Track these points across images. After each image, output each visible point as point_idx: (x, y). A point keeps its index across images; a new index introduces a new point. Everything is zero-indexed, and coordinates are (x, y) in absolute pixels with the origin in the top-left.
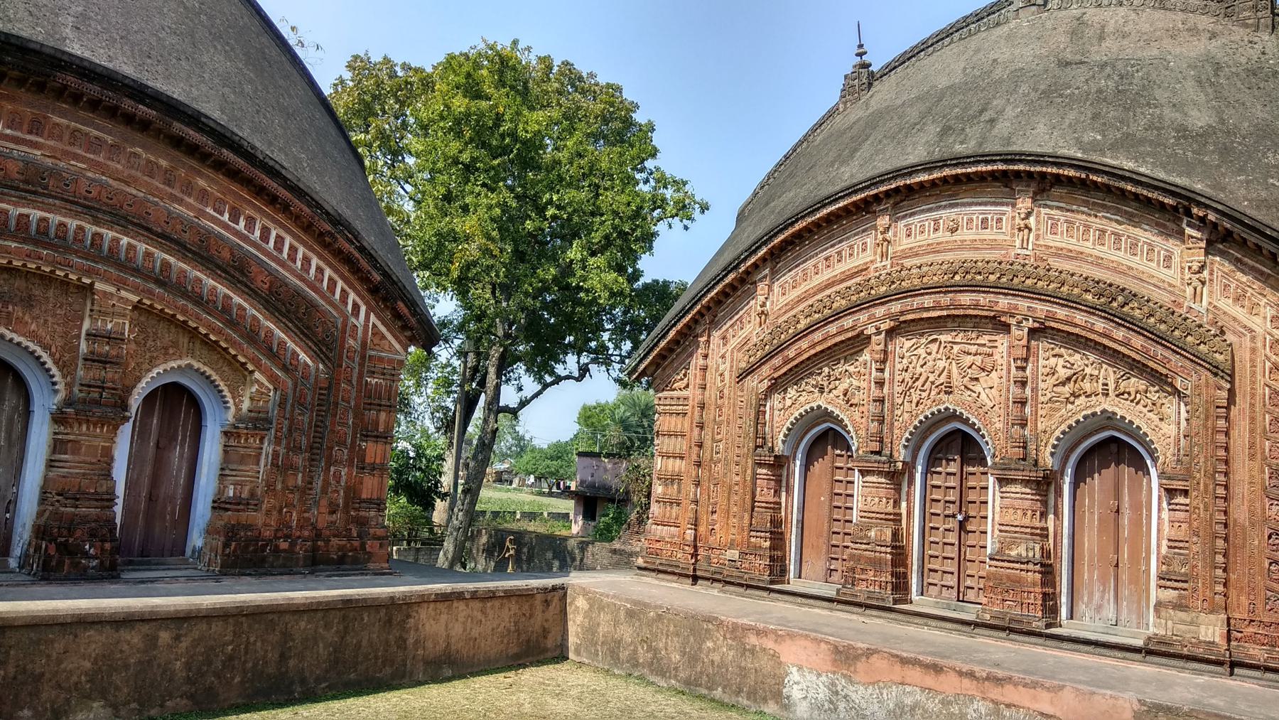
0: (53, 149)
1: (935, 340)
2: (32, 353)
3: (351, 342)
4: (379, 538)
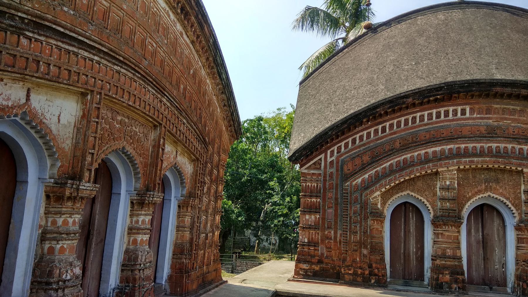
0: (497, 118)
2: (502, 201)
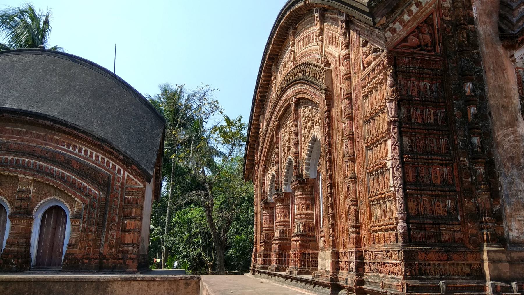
3: (117, 183)
4: (132, 259)
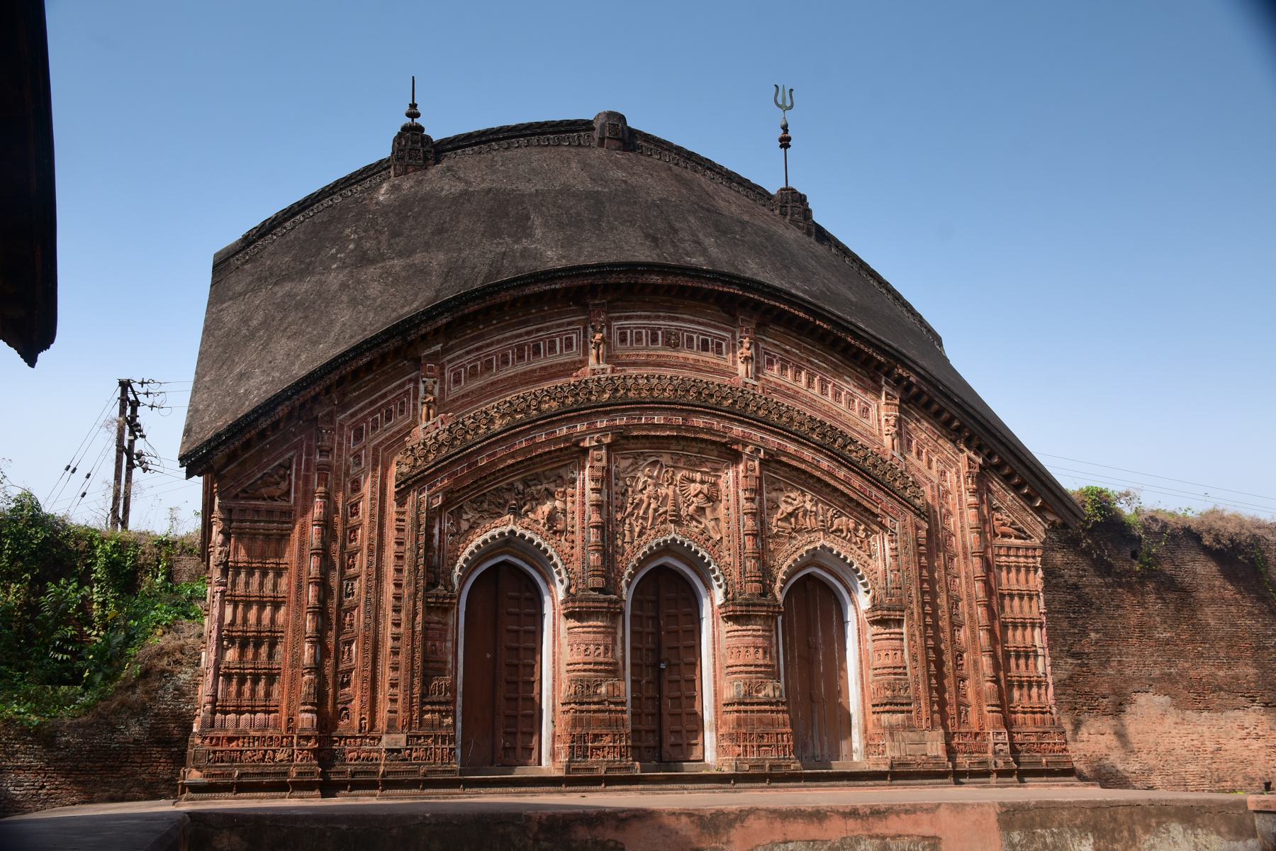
1: (654, 464)
